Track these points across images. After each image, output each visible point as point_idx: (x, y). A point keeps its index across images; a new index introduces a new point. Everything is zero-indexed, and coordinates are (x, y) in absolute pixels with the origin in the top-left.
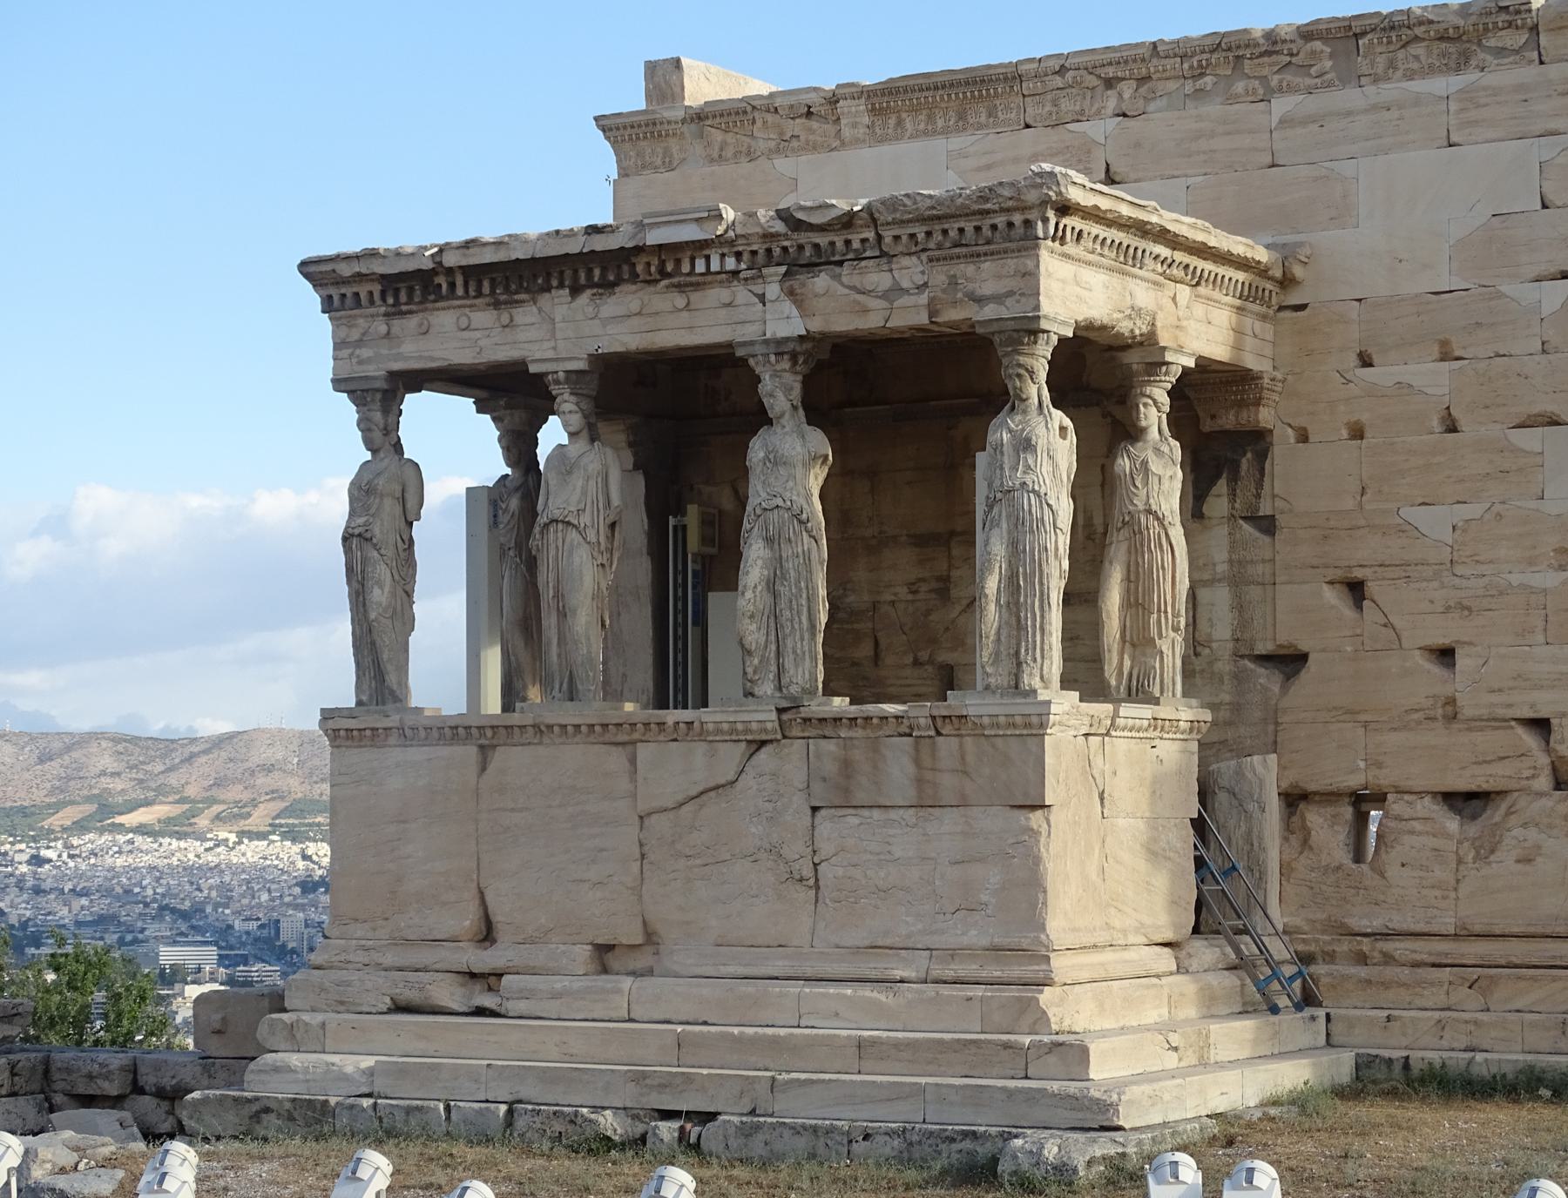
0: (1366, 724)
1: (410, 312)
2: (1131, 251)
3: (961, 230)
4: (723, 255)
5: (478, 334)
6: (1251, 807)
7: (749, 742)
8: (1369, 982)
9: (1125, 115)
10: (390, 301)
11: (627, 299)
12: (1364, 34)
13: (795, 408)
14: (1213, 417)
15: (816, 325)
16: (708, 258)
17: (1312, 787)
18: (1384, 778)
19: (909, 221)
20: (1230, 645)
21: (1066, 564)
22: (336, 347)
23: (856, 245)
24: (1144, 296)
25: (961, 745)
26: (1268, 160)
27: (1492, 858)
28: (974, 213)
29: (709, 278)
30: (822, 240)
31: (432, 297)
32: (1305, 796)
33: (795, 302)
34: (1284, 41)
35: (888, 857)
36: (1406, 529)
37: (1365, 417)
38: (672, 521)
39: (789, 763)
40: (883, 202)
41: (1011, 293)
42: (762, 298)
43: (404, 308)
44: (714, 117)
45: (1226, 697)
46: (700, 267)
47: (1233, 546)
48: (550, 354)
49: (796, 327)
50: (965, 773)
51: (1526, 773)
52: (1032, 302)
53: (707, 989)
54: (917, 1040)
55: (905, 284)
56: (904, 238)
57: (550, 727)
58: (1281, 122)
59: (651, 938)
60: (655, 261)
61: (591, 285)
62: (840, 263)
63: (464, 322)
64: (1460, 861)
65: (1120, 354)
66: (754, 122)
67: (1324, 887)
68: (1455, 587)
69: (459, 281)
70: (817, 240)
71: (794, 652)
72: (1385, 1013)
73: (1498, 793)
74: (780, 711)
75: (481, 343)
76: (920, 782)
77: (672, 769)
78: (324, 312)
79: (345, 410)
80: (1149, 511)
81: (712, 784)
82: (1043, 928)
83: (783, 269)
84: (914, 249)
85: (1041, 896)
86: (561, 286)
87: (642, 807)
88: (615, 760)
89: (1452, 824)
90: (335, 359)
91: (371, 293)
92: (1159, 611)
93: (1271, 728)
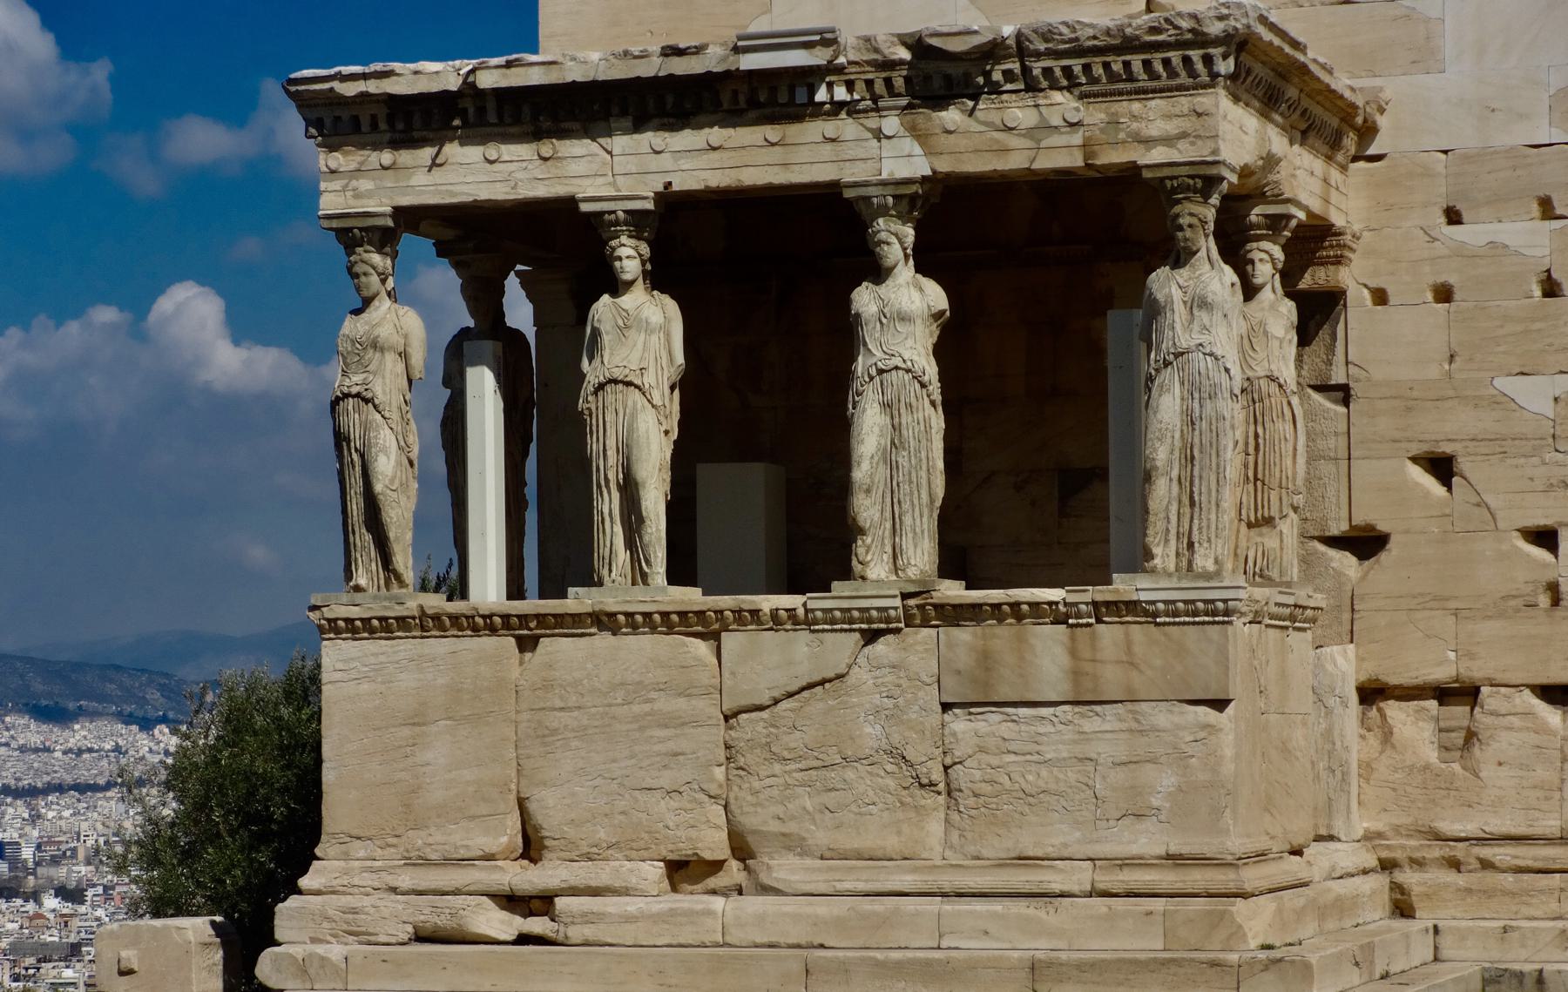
0: (1456, 613)
4: (830, 86)
5: (512, 167)
7: (861, 631)
8: (1469, 891)
10: (400, 126)
13: (906, 257)
15: (944, 166)
17: (1393, 680)
18: (1475, 671)
23: (997, 76)
24: (1278, 143)
25: (1127, 634)
35: (1036, 758)
36: (1503, 402)
37: (1452, 280)
41: (1184, 135)
42: (878, 135)
43: (416, 134)
46: (801, 97)
49: (920, 167)
50: (1132, 664)
52: (1210, 144)
53: (822, 908)
54: (1103, 961)
55: (1056, 121)
56: (1058, 72)
59: (742, 849)
67: (1409, 789)
68: (1558, 464)
69: (491, 105)
72: (1501, 923)
74: (905, 596)
75: (520, 175)
80: (1272, 378)
81: (817, 678)
86: (624, 113)
88: (702, 648)
91: (374, 118)
93: (1347, 616)
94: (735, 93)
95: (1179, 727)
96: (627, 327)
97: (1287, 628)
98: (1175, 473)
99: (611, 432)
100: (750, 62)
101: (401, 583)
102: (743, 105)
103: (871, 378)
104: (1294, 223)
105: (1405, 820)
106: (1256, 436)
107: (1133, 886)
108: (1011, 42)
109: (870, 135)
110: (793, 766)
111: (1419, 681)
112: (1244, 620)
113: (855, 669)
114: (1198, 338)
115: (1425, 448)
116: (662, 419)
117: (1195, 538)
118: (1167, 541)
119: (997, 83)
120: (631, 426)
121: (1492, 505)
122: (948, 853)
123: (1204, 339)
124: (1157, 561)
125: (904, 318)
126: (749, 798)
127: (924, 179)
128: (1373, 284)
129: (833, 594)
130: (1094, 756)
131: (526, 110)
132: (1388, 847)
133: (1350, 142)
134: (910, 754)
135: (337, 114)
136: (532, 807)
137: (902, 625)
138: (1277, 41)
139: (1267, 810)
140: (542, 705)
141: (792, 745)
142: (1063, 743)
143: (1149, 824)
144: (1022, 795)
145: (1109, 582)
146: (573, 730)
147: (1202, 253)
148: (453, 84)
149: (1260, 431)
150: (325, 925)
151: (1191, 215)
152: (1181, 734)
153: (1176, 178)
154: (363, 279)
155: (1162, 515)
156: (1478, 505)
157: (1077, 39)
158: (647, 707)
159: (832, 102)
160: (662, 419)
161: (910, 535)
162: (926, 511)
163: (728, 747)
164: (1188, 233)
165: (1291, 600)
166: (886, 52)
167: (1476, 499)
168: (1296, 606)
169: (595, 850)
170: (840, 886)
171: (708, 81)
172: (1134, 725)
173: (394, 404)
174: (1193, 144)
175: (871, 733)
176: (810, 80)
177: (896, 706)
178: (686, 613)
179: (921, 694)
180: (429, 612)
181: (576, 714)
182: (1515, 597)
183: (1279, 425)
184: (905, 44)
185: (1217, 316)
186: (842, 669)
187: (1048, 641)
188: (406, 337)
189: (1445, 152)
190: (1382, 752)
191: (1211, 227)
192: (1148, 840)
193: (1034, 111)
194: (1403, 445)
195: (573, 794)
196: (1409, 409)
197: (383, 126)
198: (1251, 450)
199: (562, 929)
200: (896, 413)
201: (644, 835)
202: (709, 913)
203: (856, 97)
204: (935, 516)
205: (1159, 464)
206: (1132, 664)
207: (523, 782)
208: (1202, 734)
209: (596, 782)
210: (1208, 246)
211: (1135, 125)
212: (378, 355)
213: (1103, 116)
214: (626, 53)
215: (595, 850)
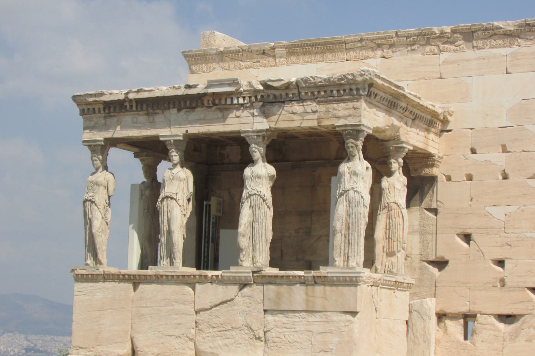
1: (114, 116)
2: (393, 103)
4: (238, 98)
6: (425, 318)
7: (240, 284)
9: (384, 57)
10: (107, 111)
11: (199, 112)
12: (475, 32)
14: (416, 170)
15: (273, 125)
16: (232, 99)
17: (448, 311)
18: (475, 308)
19: (312, 87)
20: (419, 256)
21: (367, 220)
24: (396, 123)
26: (439, 76)
27: (516, 340)
29: (232, 106)
31: (123, 111)
34: (446, 33)
38: (205, 203)
39: (256, 291)
40: (302, 79)
41: (350, 115)
43: (112, 114)
44: (227, 53)
45: (417, 276)
46: (229, 102)
47: (421, 218)
50: (326, 298)
51: (530, 308)
52: (358, 119)
56: (309, 94)
57: (162, 276)
58: (443, 62)
60: (211, 99)
61: (186, 108)
63: (135, 120)
64: (504, 341)
65: (385, 143)
66: (243, 55)
67: (452, 349)
69: (134, 104)
71: (260, 250)
73: (519, 315)
74: (253, 272)
76: (307, 301)
77: (209, 293)
78: (80, 115)
80: (395, 203)
81: (225, 299)
83: (261, 103)
84: (313, 98)
86: (174, 107)
87: (197, 307)
89: (502, 326)
91: (99, 108)
93: (433, 288)
94: (209, 100)
96: (173, 179)
97: (394, 289)
98: (343, 232)
99: (165, 214)
100: (211, 90)
101: (101, 264)
102: (211, 105)
103: (247, 198)
104: (407, 150)
106: (389, 223)
108: (294, 83)
109: (250, 115)
110: (216, 330)
111: (457, 312)
112: (367, 284)
113: (237, 297)
114: (352, 185)
115: (462, 230)
117: (350, 255)
118: (340, 256)
120: (172, 211)
121: (483, 251)
123: (354, 186)
124: (337, 263)
125: (259, 177)
127: (267, 130)
129: (231, 271)
130: (312, 330)
131: (145, 106)
135: (89, 107)
136: (135, 340)
137: (252, 282)
141: (216, 322)
144: (288, 342)
145: (319, 269)
146: (148, 314)
147: (357, 156)
148: (122, 97)
149: (391, 221)
151: (352, 143)
153: (347, 130)
154: (95, 162)
155: (339, 247)
156: (478, 251)
157: (315, 82)
158: (171, 308)
159: (238, 104)
161: (258, 252)
162: (264, 244)
163: (196, 322)
164: (351, 149)
165: (394, 280)
166: (255, 87)
167: (478, 249)
172: (326, 320)
173: (102, 203)
174: (353, 118)
175: (240, 320)
176: (231, 96)
177: (249, 310)
178: (184, 276)
179: (257, 306)
180: (106, 273)
181: (149, 309)
182: (489, 283)
183: (398, 219)
184: (261, 84)
185: (360, 178)
186: (233, 297)
187: (299, 290)
188: (108, 181)
189: (472, 129)
190: (443, 336)
191: (361, 147)
193: (302, 107)
196: (457, 217)
197: (102, 111)
198: (388, 228)
200: (254, 209)
201: (169, 352)
204: (269, 245)
205: (337, 229)
206: (326, 298)
208: (347, 324)
209: (155, 333)
211: (334, 112)
212: (98, 187)
213: (324, 109)
214: (174, 87)
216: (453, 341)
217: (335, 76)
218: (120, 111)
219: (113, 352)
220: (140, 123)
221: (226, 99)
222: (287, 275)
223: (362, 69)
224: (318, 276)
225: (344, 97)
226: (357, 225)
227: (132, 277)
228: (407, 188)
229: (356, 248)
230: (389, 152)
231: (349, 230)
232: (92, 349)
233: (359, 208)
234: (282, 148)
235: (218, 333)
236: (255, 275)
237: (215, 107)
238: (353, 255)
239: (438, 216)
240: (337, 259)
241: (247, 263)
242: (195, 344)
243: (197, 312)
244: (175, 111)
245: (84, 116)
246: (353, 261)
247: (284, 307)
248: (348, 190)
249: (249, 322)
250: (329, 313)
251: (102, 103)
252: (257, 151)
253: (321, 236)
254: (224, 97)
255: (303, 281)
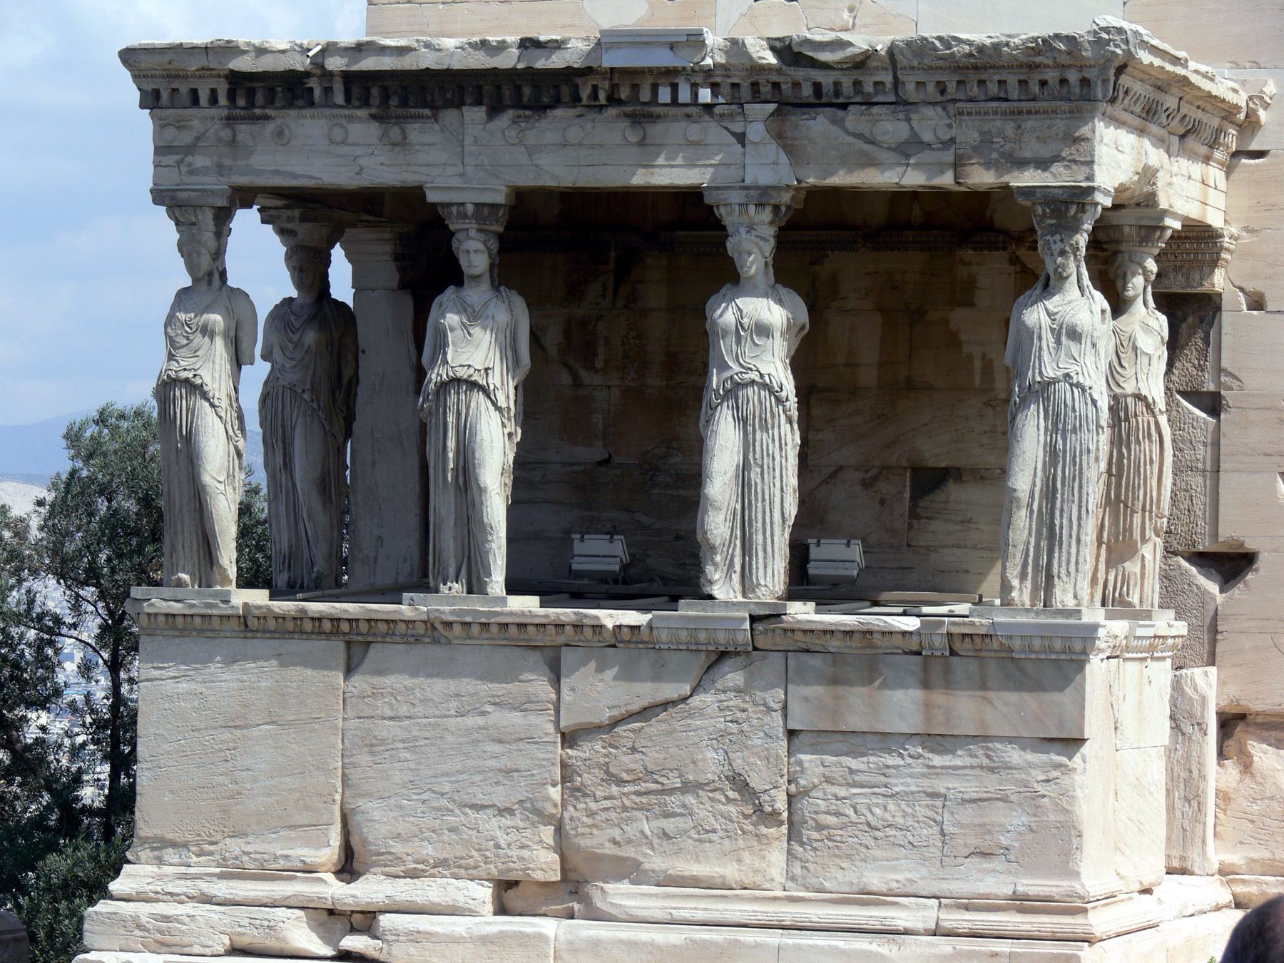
3: (1002, 83)
4: (695, 87)
10: (241, 102)
17: (1257, 706)
22: (160, 150)
23: (869, 88)
24: (1156, 156)
28: (1021, 66)
29: (673, 111)
30: (819, 76)
31: (300, 102)
32: (1242, 717)
33: (784, 147)
35: (882, 790)
42: (741, 138)
43: (258, 111)
46: (665, 95)
48: (456, 182)
52: (1085, 170)
55: (927, 136)
56: (931, 88)
57: (449, 624)
60: (606, 85)
61: (519, 105)
62: (844, 106)
67: (1268, 821)
69: (338, 87)
70: (819, 79)
74: (754, 619)
75: (364, 162)
78: (142, 106)
79: (162, 231)
80: (1139, 397)
82: (1076, 874)
83: (771, 107)
84: (939, 98)
85: (1075, 841)
86: (479, 103)
90: (156, 166)
91: (213, 92)
92: (1144, 510)
94: (595, 88)
95: (1032, 765)
97: (1145, 659)
99: (451, 433)
102: (603, 101)
104: (1169, 233)
105: (1261, 854)
107: (979, 927)
116: (506, 421)
117: (1055, 571)
119: (868, 94)
122: (790, 884)
123: (1072, 369)
124: (1015, 594)
126: (585, 819)
128: (1249, 287)
130: (943, 791)
131: (375, 92)
132: (1244, 881)
133: (1232, 139)
134: (755, 782)
138: (1157, 62)
139: (1118, 849)
140: (370, 713)
141: (632, 766)
142: (912, 776)
143: (996, 864)
146: (403, 741)
148: (300, 64)
149: (1124, 451)
150: (137, 932)
152: (1034, 772)
158: (480, 721)
160: (506, 421)
161: (761, 554)
163: (564, 765)
166: (755, 56)
168: (1155, 637)
169: (420, 866)
170: (678, 914)
171: (569, 75)
172: (985, 761)
174: (1067, 167)
178: (526, 625)
179: (767, 719)
180: (257, 612)
184: (773, 49)
190: (1241, 781)
192: (996, 883)
194: (1274, 459)
195: (401, 807)
197: (223, 101)
199: (385, 946)
200: (750, 428)
201: (474, 853)
202: (542, 938)
203: (721, 100)
204: (787, 535)
207: (348, 792)
208: (1054, 774)
209: (425, 797)
210: (1076, 269)
215: (420, 866)
216: (1272, 798)
217: (1017, 41)
218: (290, 105)
219: (286, 857)
220: (357, 145)
221: (655, 88)
222: (865, 628)
223: (1103, 24)
224: (964, 635)
225: (1039, 104)
226: (1076, 484)
227: (345, 627)
228: (1168, 349)
229: (1074, 550)
230: (1119, 242)
231: (1054, 498)
232: (212, 848)
233: (1085, 436)
234: (817, 238)
235: (637, 799)
236: (760, 627)
237: (612, 111)
238: (1063, 571)
239: (1222, 416)
240: (1015, 583)
241: (724, 588)
242: (559, 830)
243: (569, 739)
244: (479, 113)
245: (157, 111)
246: (1064, 590)
247: (855, 722)
248: (1054, 381)
249: (738, 764)
250: (998, 745)
251: (226, 77)
252: (753, 250)
253: (841, 468)
254: (650, 80)
255: (915, 648)
